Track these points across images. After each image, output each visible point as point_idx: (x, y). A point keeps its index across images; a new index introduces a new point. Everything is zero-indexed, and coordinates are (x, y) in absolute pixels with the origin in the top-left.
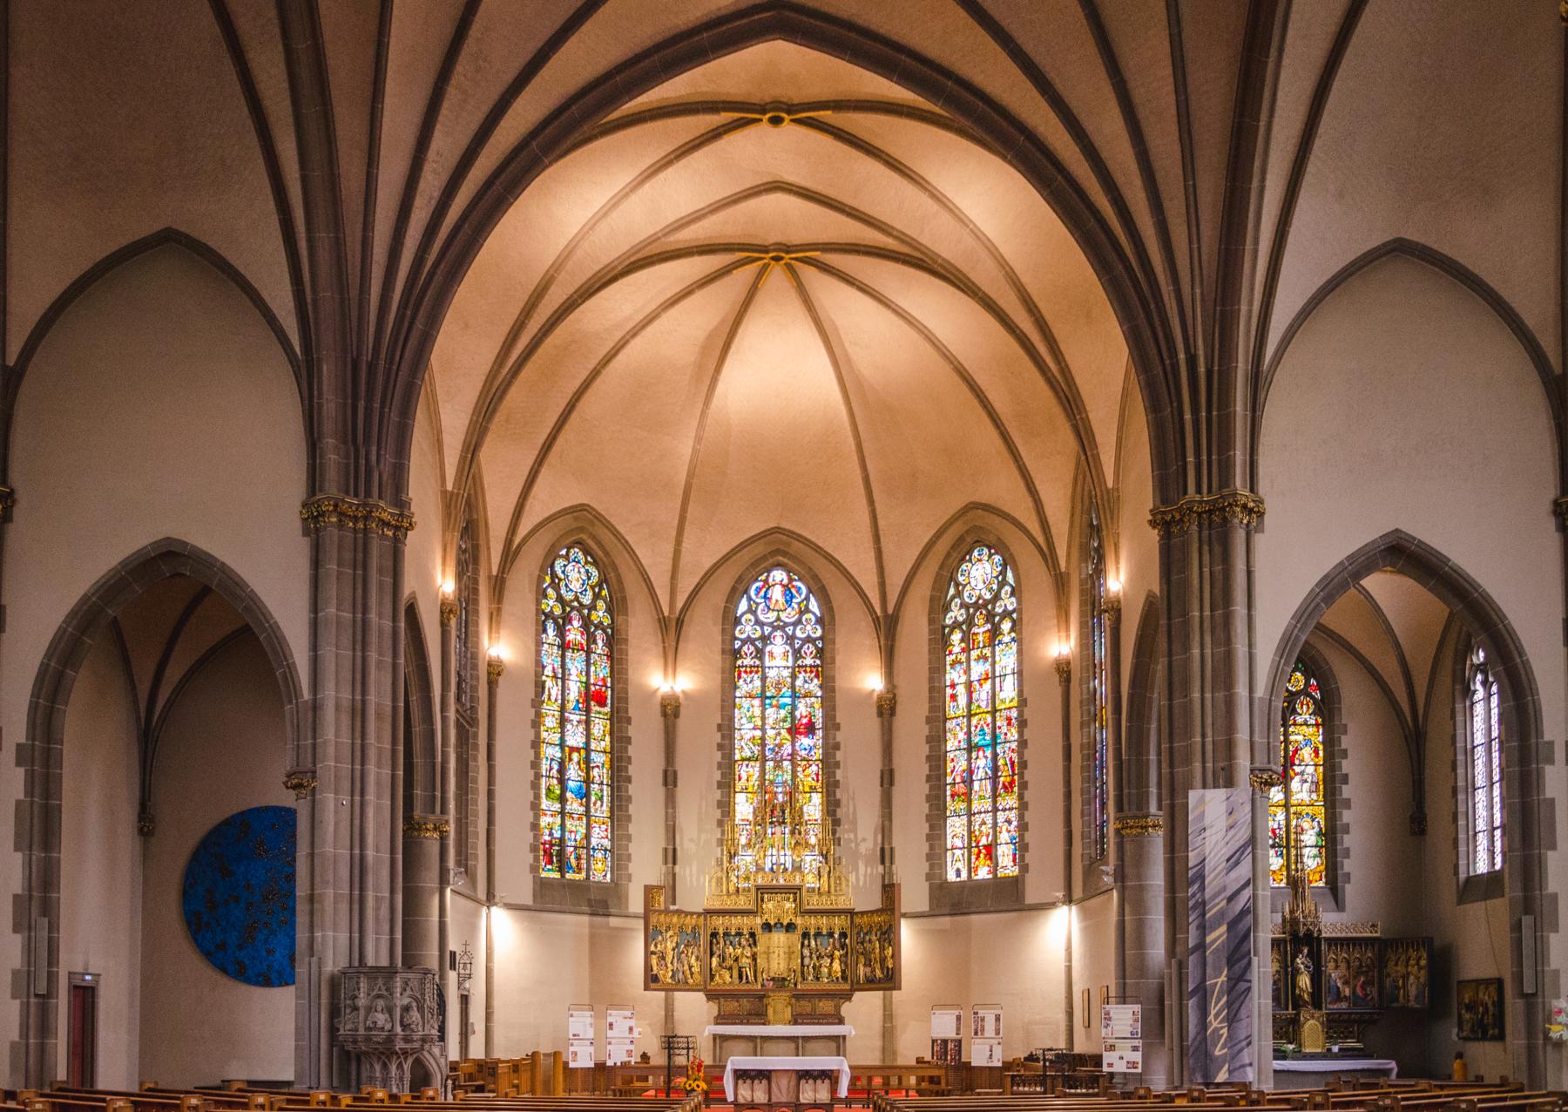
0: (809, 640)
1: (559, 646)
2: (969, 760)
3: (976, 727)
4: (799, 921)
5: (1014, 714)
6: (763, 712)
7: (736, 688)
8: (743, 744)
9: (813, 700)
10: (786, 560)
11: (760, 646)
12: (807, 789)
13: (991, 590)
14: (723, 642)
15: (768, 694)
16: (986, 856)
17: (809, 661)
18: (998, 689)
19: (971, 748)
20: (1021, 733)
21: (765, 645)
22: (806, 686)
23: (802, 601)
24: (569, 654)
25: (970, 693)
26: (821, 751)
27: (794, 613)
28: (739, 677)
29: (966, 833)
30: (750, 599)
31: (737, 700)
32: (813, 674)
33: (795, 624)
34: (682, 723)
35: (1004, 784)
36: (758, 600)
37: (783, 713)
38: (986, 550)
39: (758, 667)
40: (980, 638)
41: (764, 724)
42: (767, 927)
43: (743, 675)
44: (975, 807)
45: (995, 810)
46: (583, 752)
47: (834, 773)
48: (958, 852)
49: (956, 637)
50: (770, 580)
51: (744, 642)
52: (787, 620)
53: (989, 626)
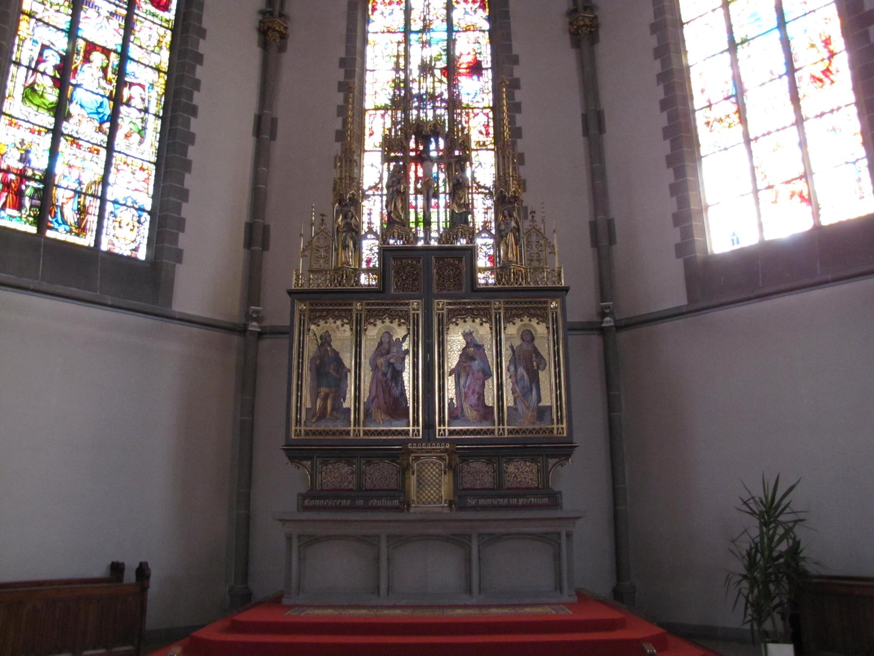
9: (477, 34)
28: (374, 9)
32: (477, 5)
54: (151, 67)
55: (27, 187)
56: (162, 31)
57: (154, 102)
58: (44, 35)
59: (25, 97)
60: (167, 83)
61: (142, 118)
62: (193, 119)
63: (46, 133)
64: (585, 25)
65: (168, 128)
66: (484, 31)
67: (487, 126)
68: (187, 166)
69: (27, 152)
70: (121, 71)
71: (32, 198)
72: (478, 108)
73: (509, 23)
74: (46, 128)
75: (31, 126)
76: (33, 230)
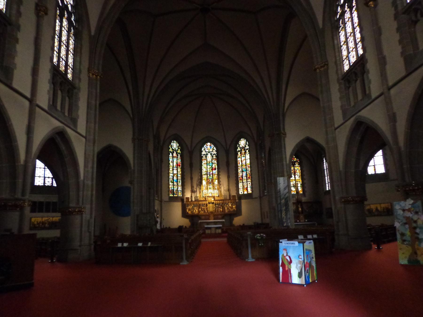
1: (172, 157)
4: (214, 202)
5: (249, 165)
6: (207, 167)
7: (202, 162)
9: (215, 164)
13: (244, 145)
17: (214, 158)
18: (246, 161)
19: (242, 171)
20: (250, 169)
21: (207, 155)
22: (214, 162)
24: (174, 158)
25: (242, 162)
30: (204, 148)
33: (212, 152)
36: (205, 148)
37: (210, 166)
38: (243, 139)
40: (243, 153)
41: (207, 168)
42: (209, 203)
43: (203, 160)
44: (244, 181)
45: (247, 182)
46: (176, 174)
49: (239, 153)
51: (203, 155)
52: (211, 151)
53: (244, 151)
59: (171, 182)
60: (181, 175)
67: (217, 177)
70: (177, 176)
76: (172, 196)
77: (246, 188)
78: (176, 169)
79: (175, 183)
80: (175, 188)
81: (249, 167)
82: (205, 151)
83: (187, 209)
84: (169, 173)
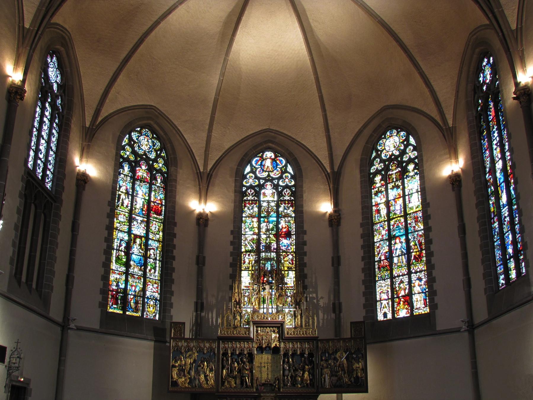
0: (287, 187)
2: (390, 246)
3: (393, 226)
7: (243, 212)
8: (246, 242)
9: (289, 218)
10: (273, 146)
11: (258, 190)
12: (286, 269)
14: (235, 186)
15: (262, 215)
16: (404, 302)
17: (287, 198)
19: (391, 238)
20: (425, 224)
22: (285, 211)
23: (283, 167)
26: (294, 247)
27: (278, 173)
28: (245, 206)
29: (389, 290)
30: (252, 166)
31: (243, 218)
34: (210, 229)
35: (415, 256)
36: (257, 167)
37: (271, 226)
39: (256, 201)
43: (247, 205)
44: (395, 273)
45: (409, 273)
47: (303, 258)
48: (384, 302)
50: (264, 156)
51: (248, 188)
52: (274, 176)
54: (156, 241)
55: (119, 296)
56: (159, 224)
57: (158, 255)
58: (121, 235)
59: (116, 262)
60: (162, 246)
61: (154, 262)
62: (174, 262)
63: (123, 274)
64: (334, 219)
65: (164, 266)
66: (292, 217)
67: (292, 260)
68: (172, 281)
69: (118, 282)
70: (146, 245)
71: (120, 300)
72: (289, 252)
73: (303, 215)
74: (123, 272)
75: (119, 272)
77: (403, 296)
78: (142, 221)
79: (135, 270)
80: (136, 286)
81: (417, 221)
82: (254, 176)
83: (174, 366)
84: (111, 228)
